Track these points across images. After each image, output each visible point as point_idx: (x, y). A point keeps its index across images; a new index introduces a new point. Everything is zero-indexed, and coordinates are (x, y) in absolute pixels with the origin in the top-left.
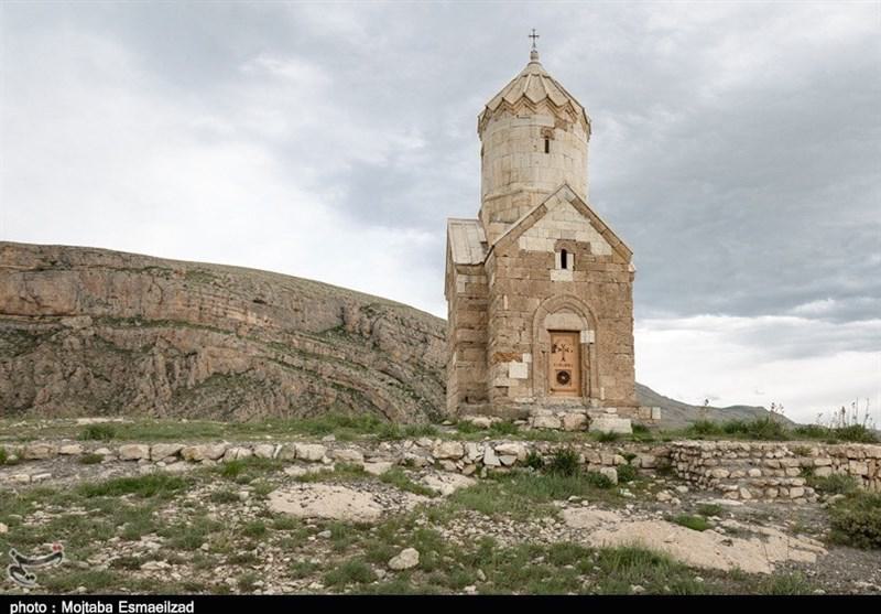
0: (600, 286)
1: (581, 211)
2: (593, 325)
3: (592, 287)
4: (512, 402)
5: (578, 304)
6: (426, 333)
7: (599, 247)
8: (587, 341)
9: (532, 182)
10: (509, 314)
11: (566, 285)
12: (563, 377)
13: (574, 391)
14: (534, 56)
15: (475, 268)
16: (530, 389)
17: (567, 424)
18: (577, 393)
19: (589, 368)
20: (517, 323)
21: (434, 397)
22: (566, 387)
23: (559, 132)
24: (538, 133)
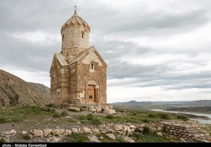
0: (100, 74)
1: (96, 54)
2: (99, 84)
3: (99, 74)
4: (80, 104)
5: (95, 78)
6: (8, 78)
7: (100, 64)
9: (79, 45)
10: (80, 80)
11: (93, 73)
12: (91, 97)
13: (93, 101)
15: (66, 67)
16: (85, 100)
17: (98, 110)
18: (94, 101)
19: (98, 95)
20: (82, 83)
21: (10, 93)
22: (91, 100)
23: (85, 32)
24: (81, 32)
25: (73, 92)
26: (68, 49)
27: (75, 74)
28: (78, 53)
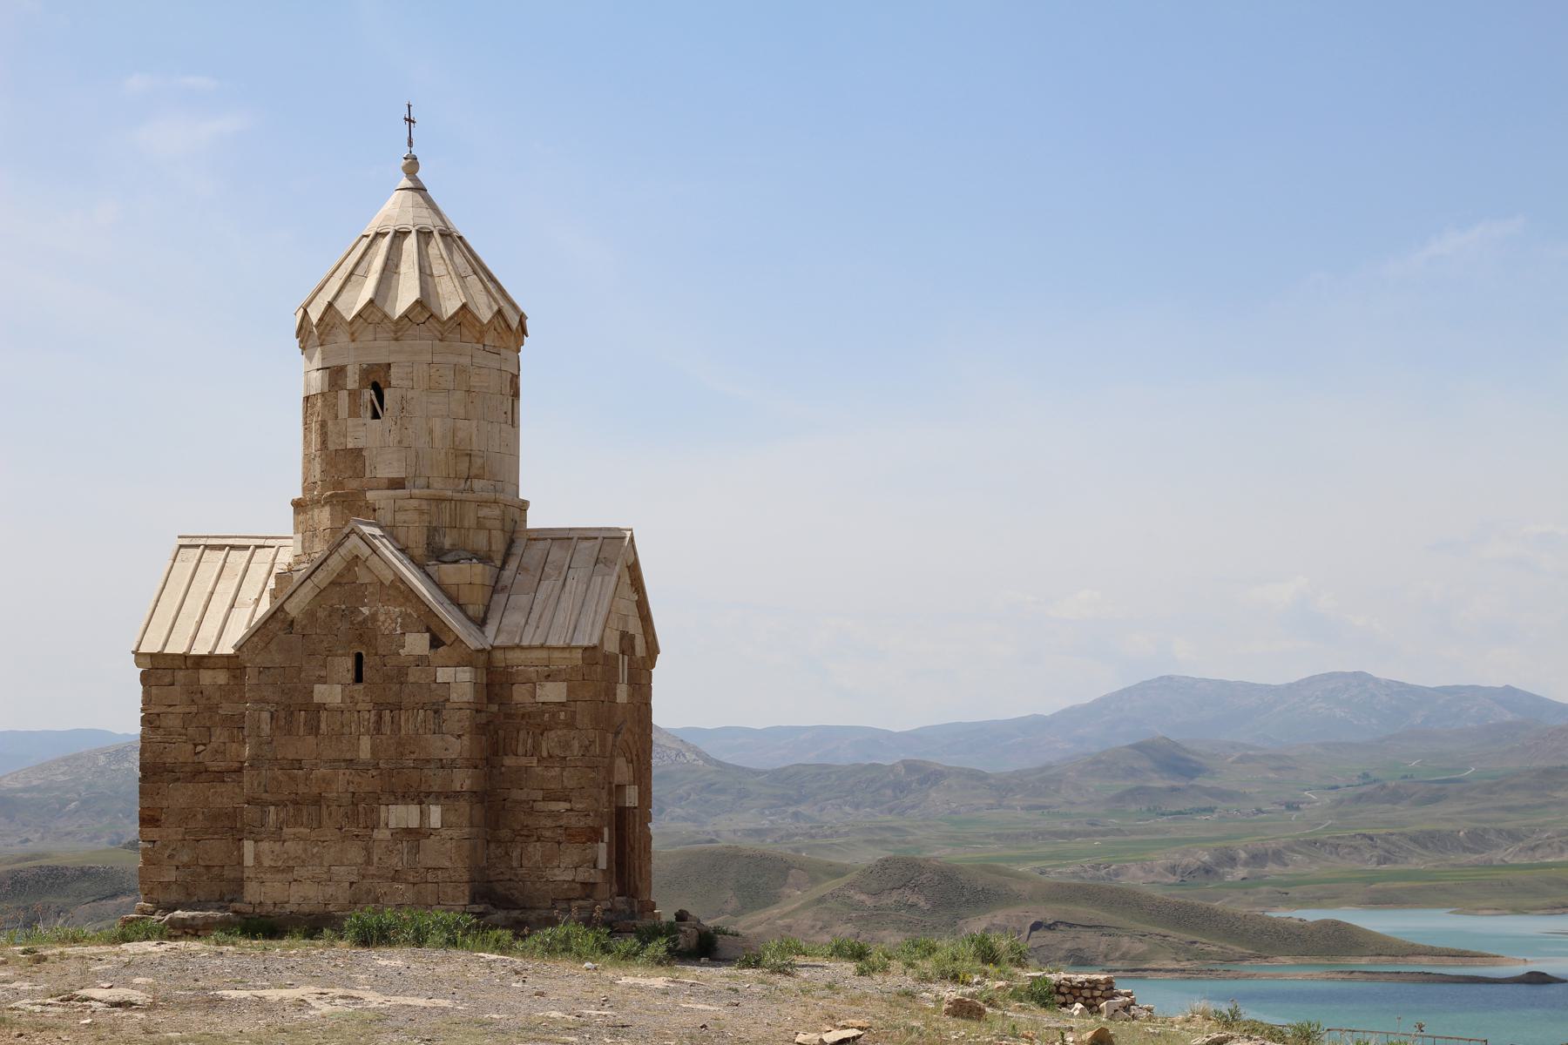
7: (640, 649)
8: (632, 805)
14: (412, 166)
19: (633, 849)
25: (548, 834)
26: (440, 500)
27: (562, 716)
28: (499, 545)
